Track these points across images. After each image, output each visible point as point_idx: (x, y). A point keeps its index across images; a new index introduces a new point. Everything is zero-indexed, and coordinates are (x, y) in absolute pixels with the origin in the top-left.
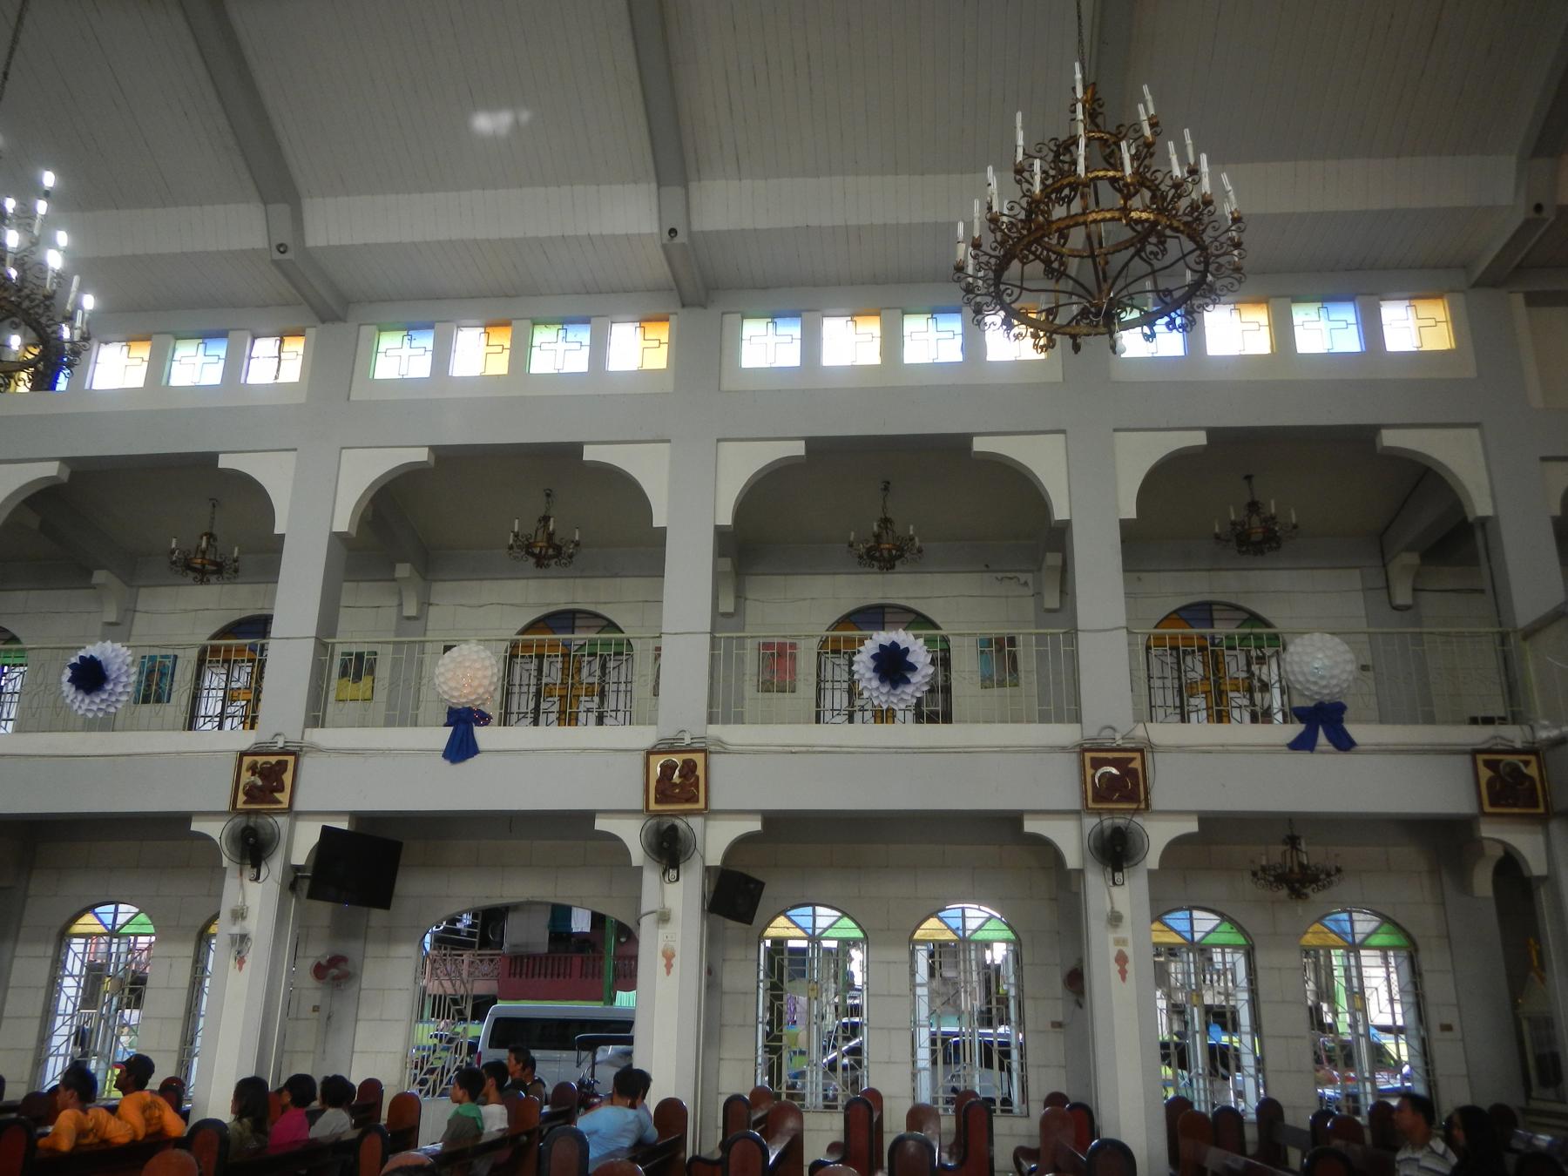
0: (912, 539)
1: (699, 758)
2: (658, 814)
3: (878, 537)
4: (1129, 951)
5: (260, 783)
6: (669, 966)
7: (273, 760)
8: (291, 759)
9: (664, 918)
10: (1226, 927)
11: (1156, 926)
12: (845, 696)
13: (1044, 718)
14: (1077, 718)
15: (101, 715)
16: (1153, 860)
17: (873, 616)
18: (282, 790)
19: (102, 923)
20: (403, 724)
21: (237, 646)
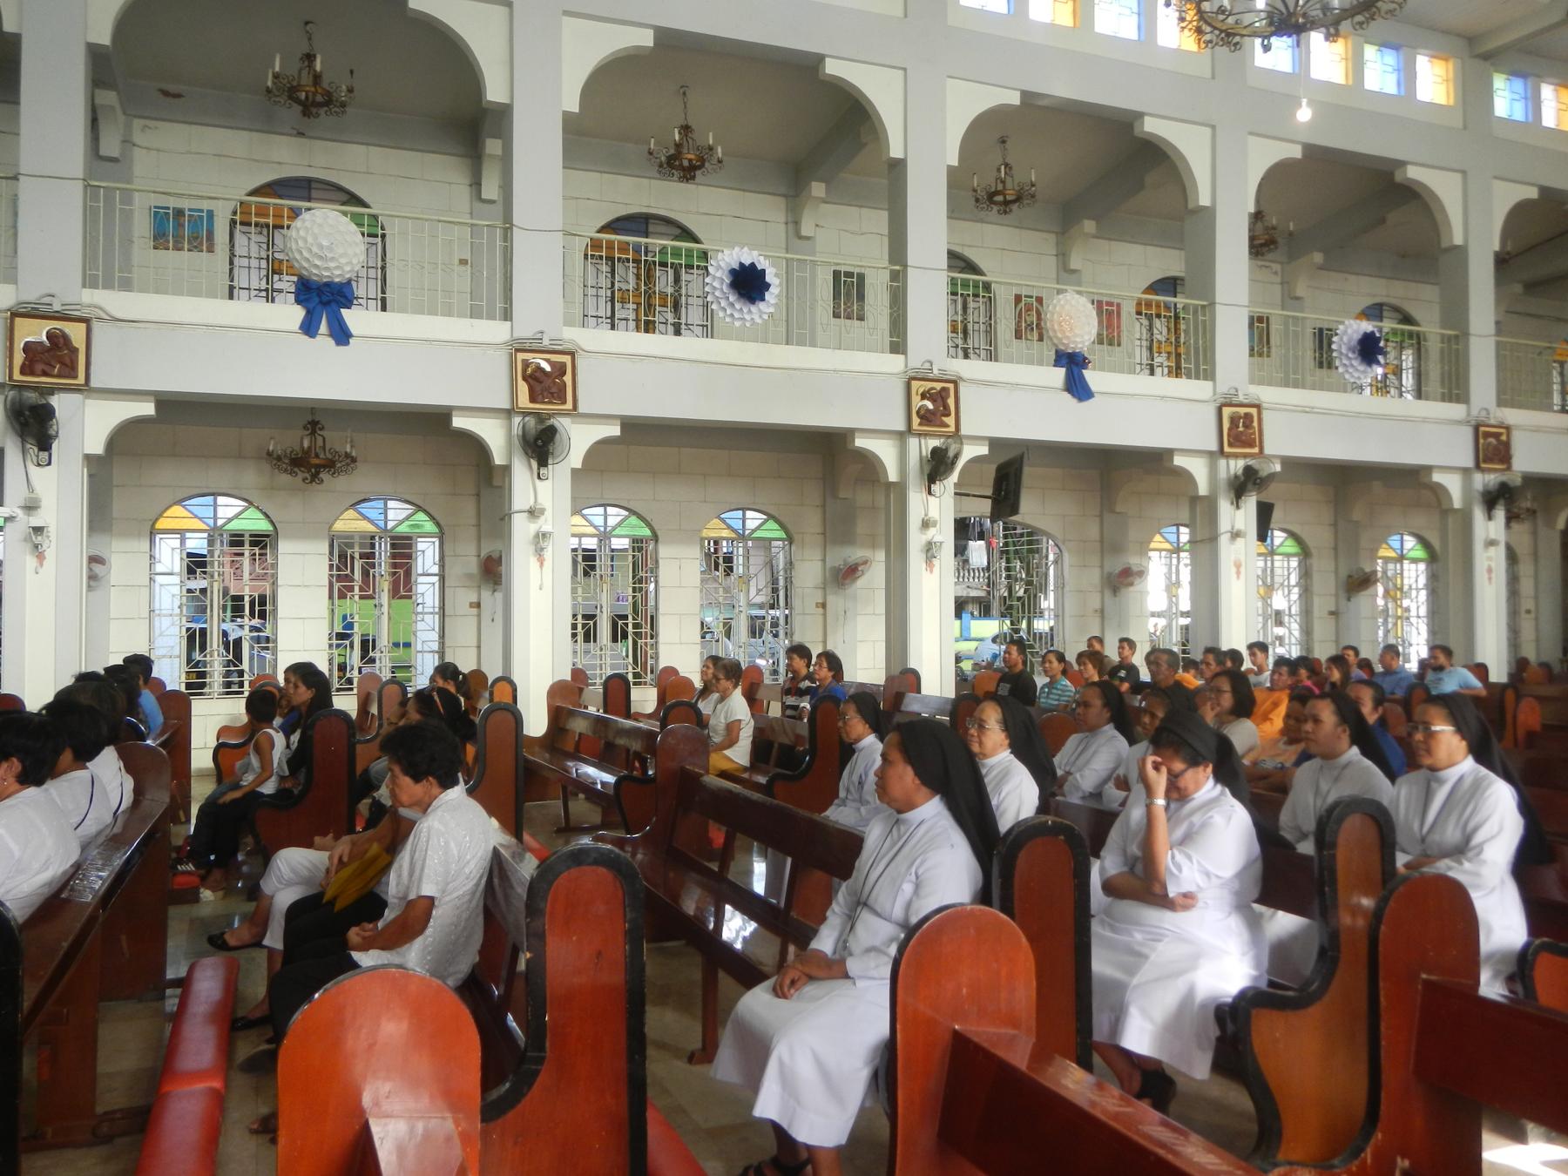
0: (711, 149)
1: (1254, 411)
2: (21, 387)
3: (678, 146)
4: (1493, 565)
5: (930, 406)
6: (1238, 573)
7: (938, 386)
8: (951, 386)
9: (1236, 535)
10: (772, 525)
11: (577, 520)
12: (1145, 353)
13: (475, 313)
14: (507, 315)
15: (737, 324)
16: (576, 458)
17: (303, 189)
18: (948, 415)
19: (592, 525)
20: (801, 343)
21: (673, 248)
